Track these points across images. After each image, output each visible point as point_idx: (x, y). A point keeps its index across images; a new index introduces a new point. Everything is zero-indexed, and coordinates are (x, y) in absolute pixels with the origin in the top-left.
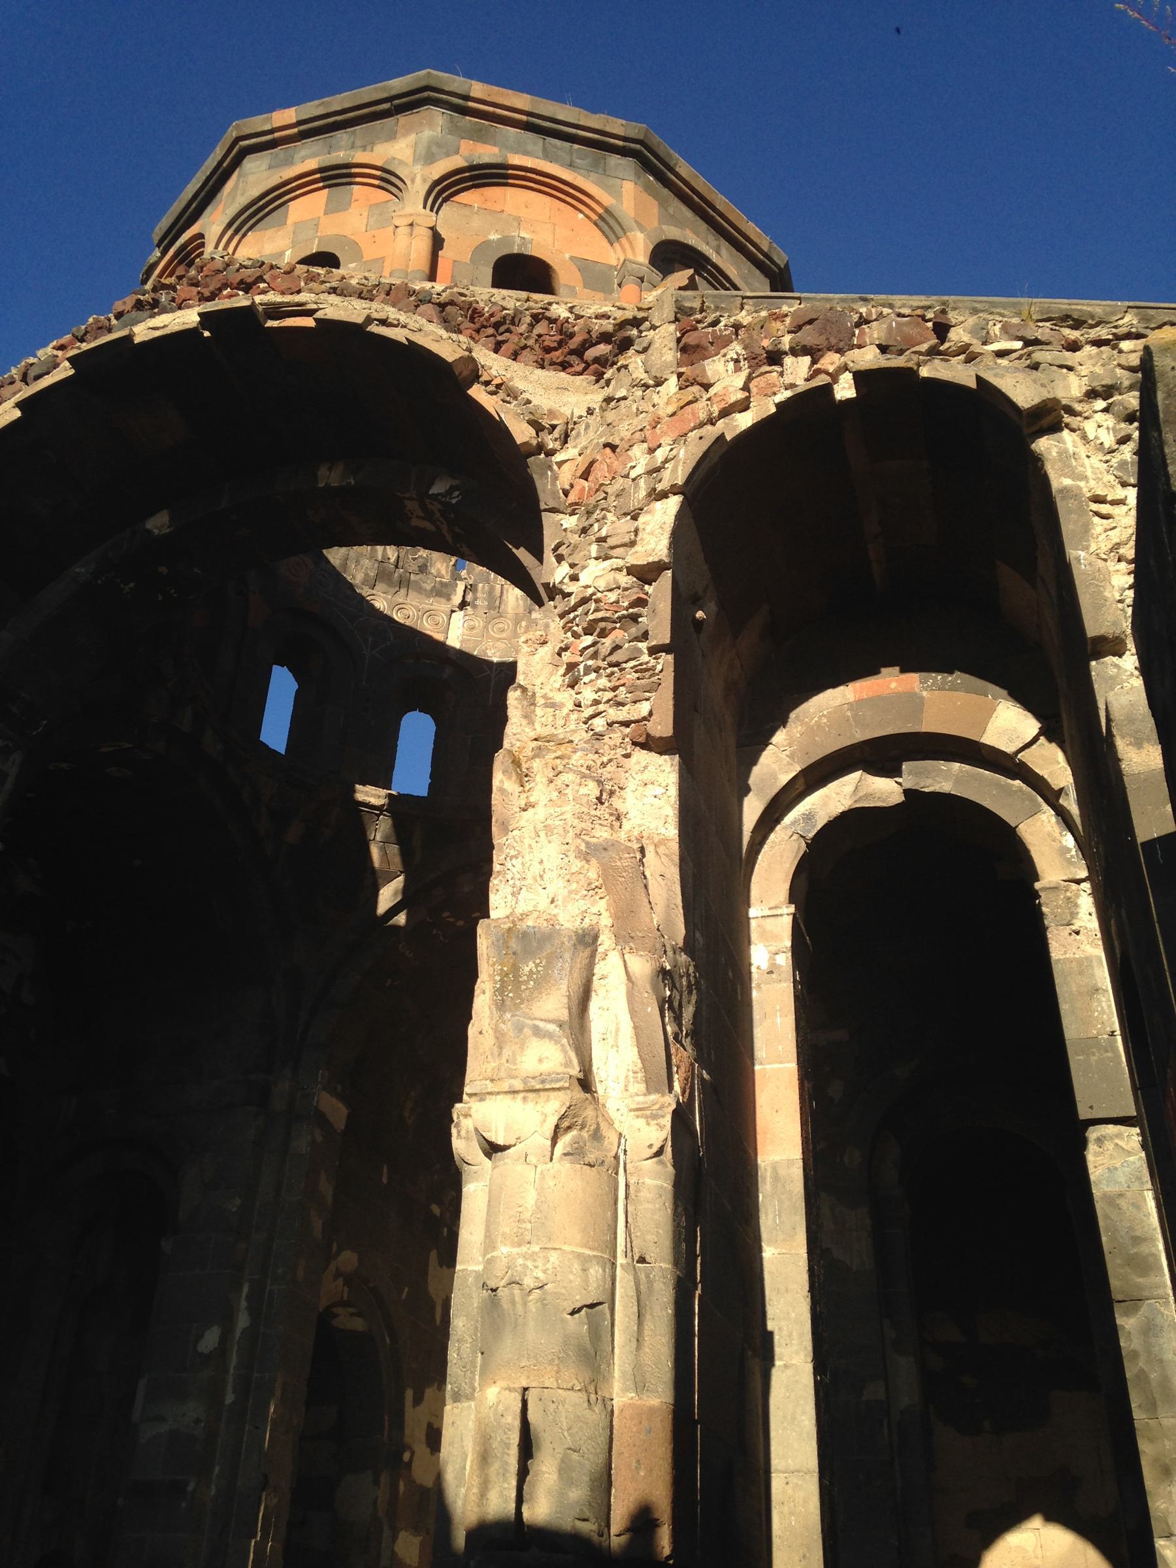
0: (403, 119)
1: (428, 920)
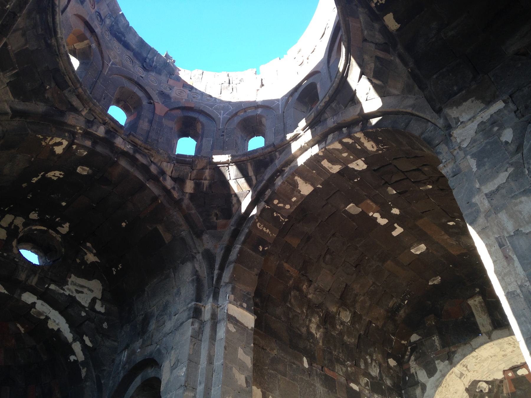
1: (267, 207)
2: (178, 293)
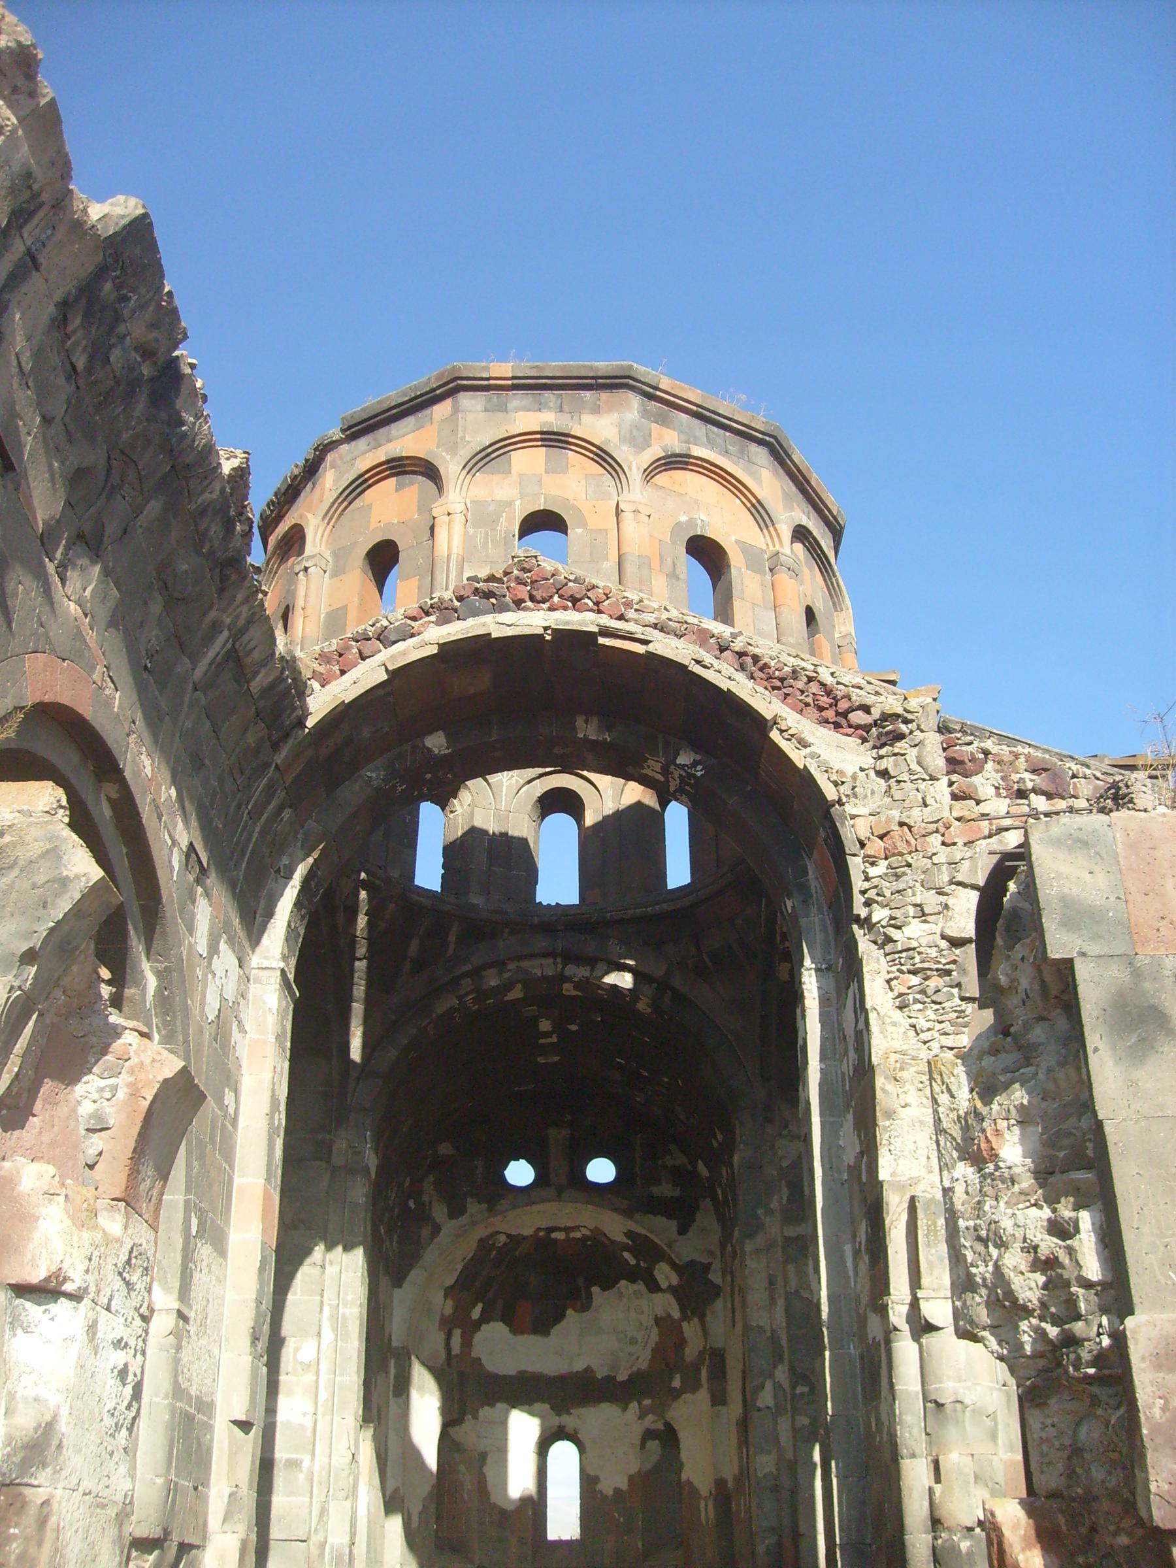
0: (604, 395)
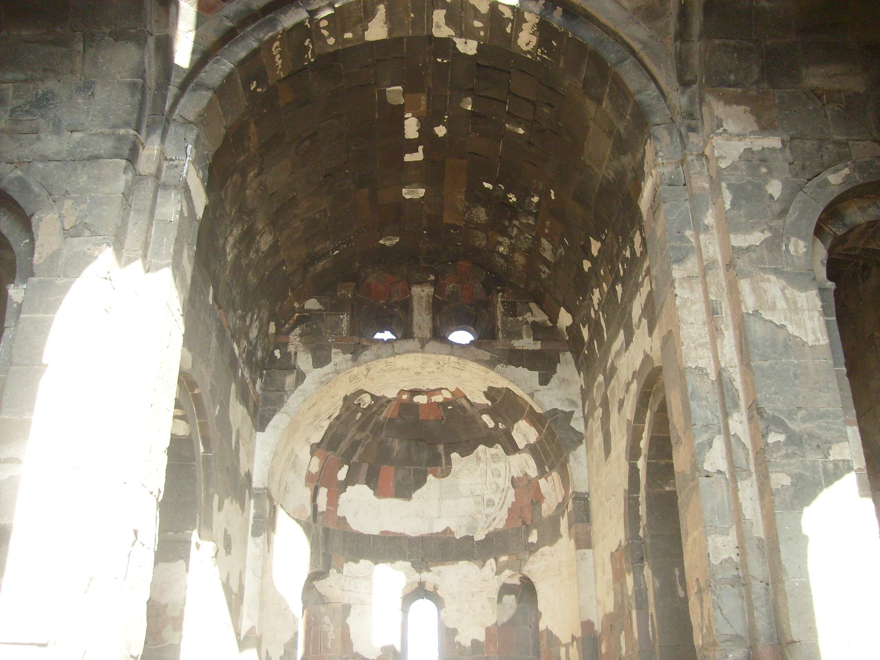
2: (87, 87)
